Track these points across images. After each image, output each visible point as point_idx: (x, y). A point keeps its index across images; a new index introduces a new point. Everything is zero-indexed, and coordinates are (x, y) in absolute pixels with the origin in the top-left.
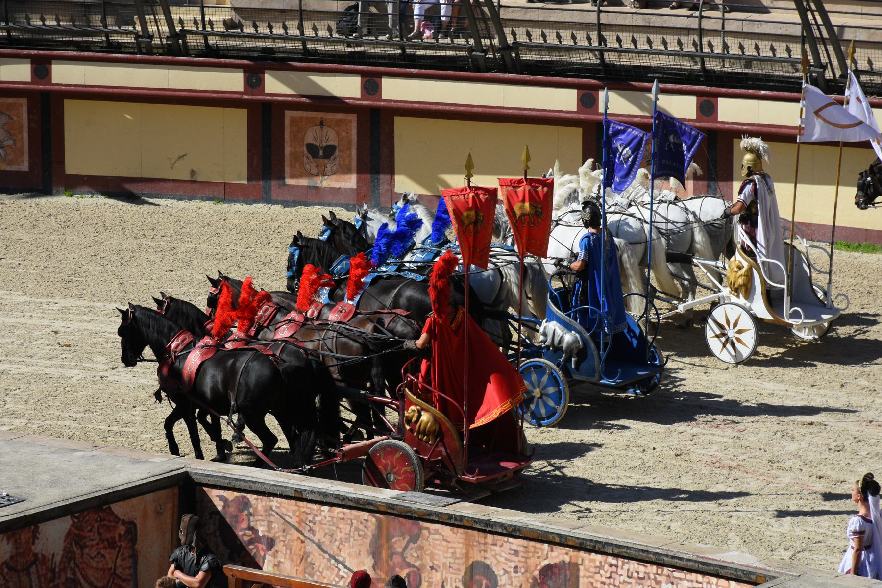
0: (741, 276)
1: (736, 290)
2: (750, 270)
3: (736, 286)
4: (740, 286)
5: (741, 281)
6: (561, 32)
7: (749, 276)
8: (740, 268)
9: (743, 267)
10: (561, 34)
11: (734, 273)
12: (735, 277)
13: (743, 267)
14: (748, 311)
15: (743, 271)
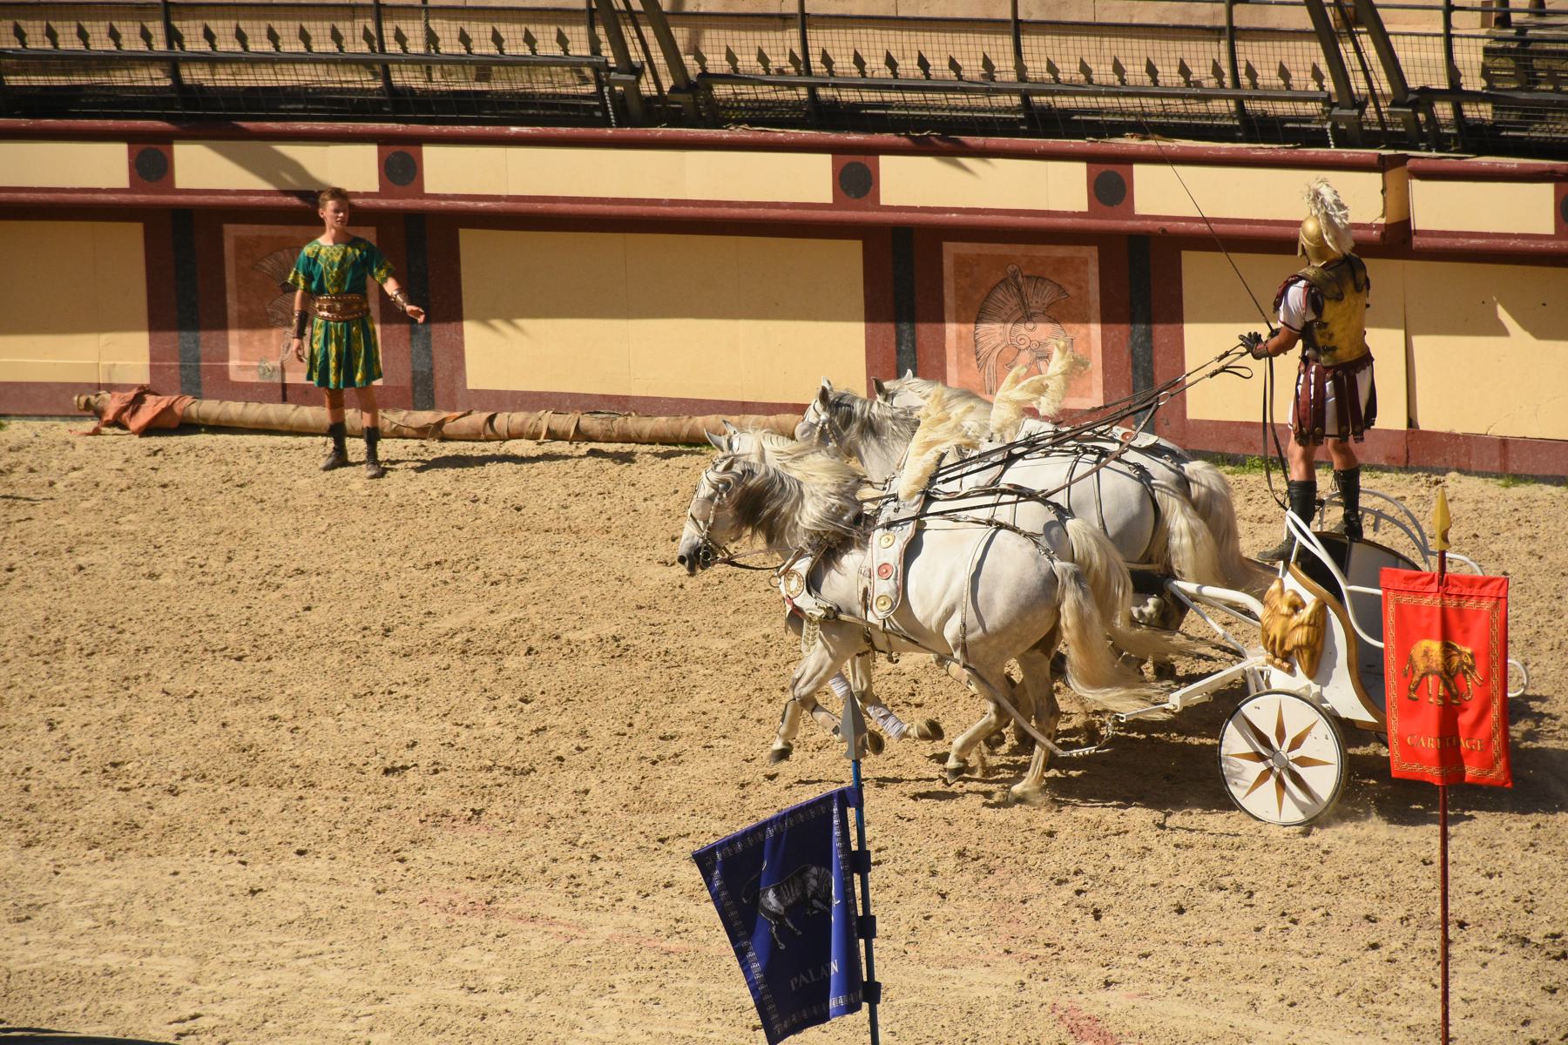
0: (1301, 625)
1: (1285, 656)
2: (1321, 609)
3: (1287, 647)
4: (1299, 647)
5: (1300, 636)
6: (86, 24)
7: (1319, 624)
8: (1296, 607)
9: (1304, 605)
10: (88, 30)
11: (1283, 619)
12: (1284, 629)
13: (1304, 605)
14: (1317, 704)
15: (1305, 614)
